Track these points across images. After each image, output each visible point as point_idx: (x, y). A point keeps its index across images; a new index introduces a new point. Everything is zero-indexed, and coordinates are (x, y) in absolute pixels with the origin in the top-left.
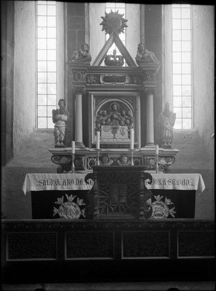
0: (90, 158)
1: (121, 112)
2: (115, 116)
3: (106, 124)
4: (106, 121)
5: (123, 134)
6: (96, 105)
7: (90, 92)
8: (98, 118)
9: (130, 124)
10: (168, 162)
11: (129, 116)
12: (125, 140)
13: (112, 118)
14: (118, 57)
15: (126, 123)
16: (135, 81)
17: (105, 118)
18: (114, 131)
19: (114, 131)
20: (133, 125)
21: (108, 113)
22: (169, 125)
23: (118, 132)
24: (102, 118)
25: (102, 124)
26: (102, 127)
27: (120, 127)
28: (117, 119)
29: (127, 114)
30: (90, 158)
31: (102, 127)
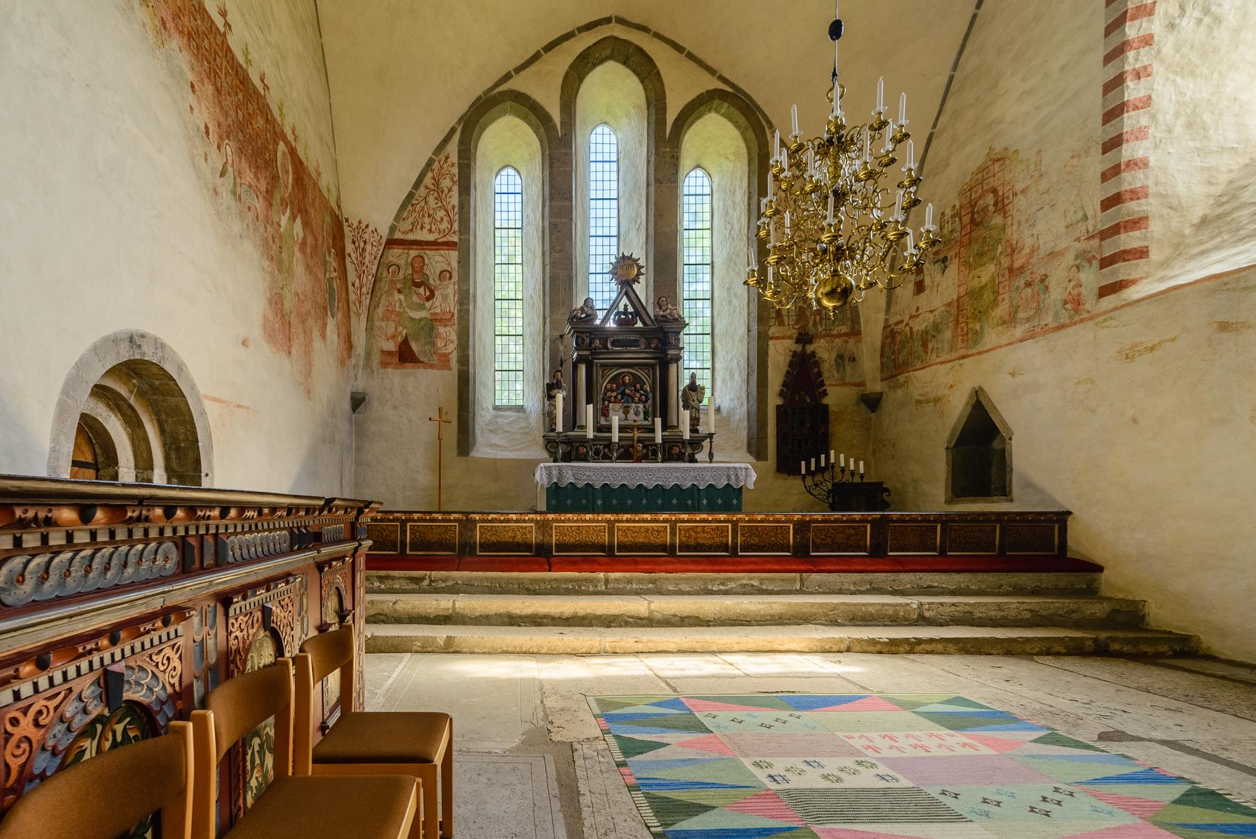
0: (594, 445)
1: (635, 386)
2: (627, 391)
3: (614, 402)
4: (616, 397)
5: (637, 413)
6: (603, 377)
7: (595, 361)
8: (605, 394)
9: (646, 401)
10: (694, 450)
11: (646, 391)
12: (639, 423)
13: (623, 393)
14: (631, 313)
15: (640, 401)
16: (653, 346)
17: (614, 394)
18: (626, 412)
19: (626, 412)
20: (649, 402)
21: (618, 388)
22: (696, 402)
23: (632, 411)
24: (609, 394)
25: (610, 402)
26: (611, 405)
27: (634, 405)
28: (628, 395)
29: (642, 389)
30: (594, 445)
31: (611, 405)
